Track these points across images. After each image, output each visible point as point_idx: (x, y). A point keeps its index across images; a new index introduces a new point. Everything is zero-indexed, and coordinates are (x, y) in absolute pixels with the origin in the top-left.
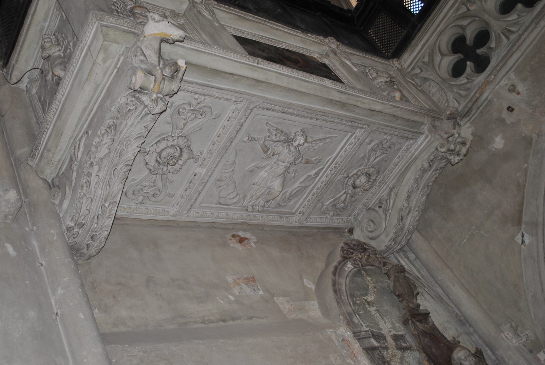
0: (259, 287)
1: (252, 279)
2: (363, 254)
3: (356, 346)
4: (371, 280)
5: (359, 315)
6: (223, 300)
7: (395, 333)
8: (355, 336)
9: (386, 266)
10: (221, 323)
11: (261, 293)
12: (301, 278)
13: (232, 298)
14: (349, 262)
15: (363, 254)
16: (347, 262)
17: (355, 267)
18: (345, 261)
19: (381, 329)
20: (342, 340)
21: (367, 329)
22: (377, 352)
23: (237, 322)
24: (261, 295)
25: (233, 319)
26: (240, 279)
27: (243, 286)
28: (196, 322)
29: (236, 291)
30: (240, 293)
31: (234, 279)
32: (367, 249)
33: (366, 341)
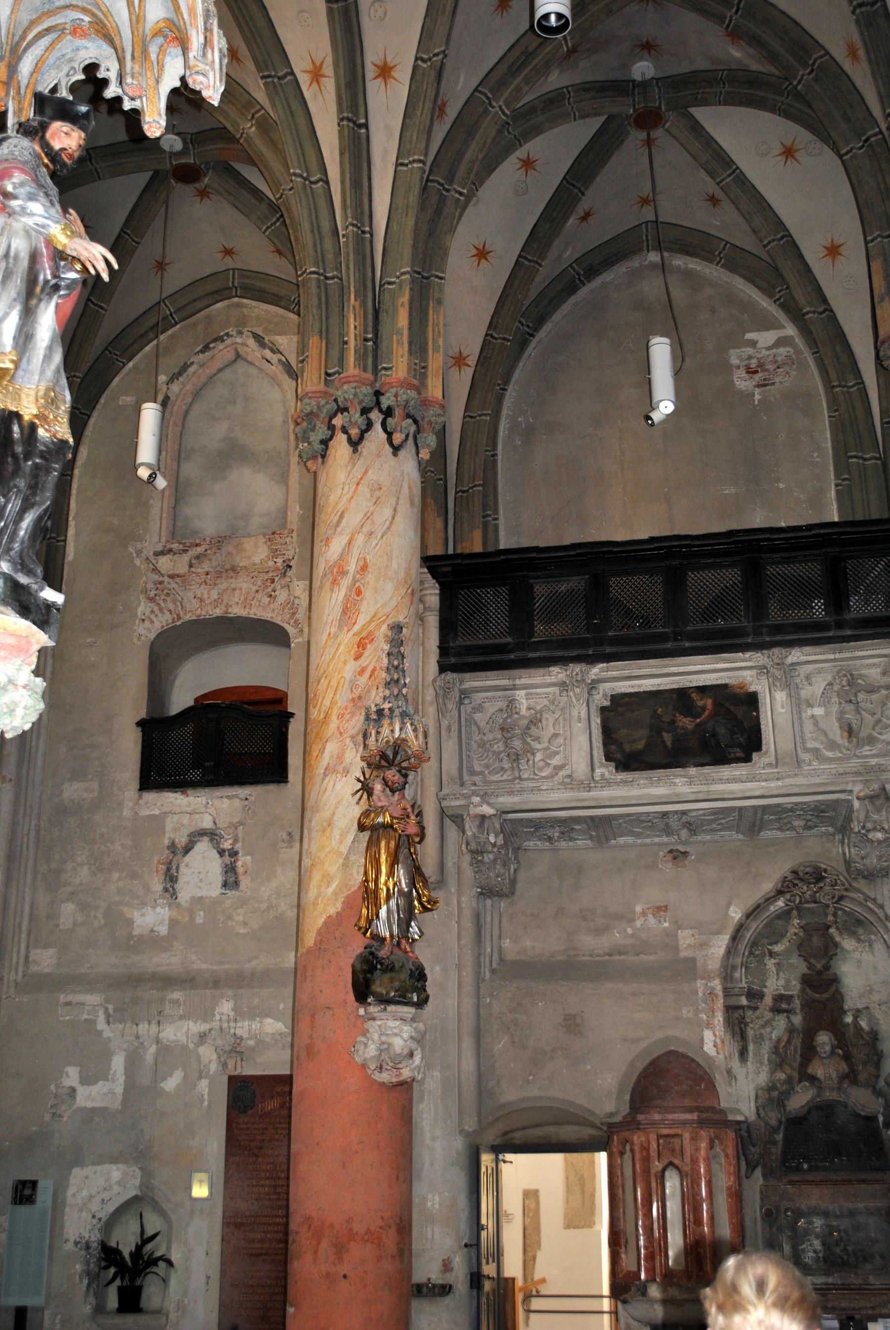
3: (720, 1003)
5: (746, 969)
6: (619, 933)
7: (783, 992)
8: (724, 992)
9: (842, 903)
10: (607, 958)
11: (666, 925)
12: (729, 905)
13: (629, 931)
19: (765, 987)
20: (710, 994)
21: (745, 986)
22: (741, 1012)
23: (622, 957)
24: (665, 928)
25: (620, 954)
27: (650, 917)
28: (584, 955)
29: (638, 924)
32: (825, 878)
33: (734, 998)
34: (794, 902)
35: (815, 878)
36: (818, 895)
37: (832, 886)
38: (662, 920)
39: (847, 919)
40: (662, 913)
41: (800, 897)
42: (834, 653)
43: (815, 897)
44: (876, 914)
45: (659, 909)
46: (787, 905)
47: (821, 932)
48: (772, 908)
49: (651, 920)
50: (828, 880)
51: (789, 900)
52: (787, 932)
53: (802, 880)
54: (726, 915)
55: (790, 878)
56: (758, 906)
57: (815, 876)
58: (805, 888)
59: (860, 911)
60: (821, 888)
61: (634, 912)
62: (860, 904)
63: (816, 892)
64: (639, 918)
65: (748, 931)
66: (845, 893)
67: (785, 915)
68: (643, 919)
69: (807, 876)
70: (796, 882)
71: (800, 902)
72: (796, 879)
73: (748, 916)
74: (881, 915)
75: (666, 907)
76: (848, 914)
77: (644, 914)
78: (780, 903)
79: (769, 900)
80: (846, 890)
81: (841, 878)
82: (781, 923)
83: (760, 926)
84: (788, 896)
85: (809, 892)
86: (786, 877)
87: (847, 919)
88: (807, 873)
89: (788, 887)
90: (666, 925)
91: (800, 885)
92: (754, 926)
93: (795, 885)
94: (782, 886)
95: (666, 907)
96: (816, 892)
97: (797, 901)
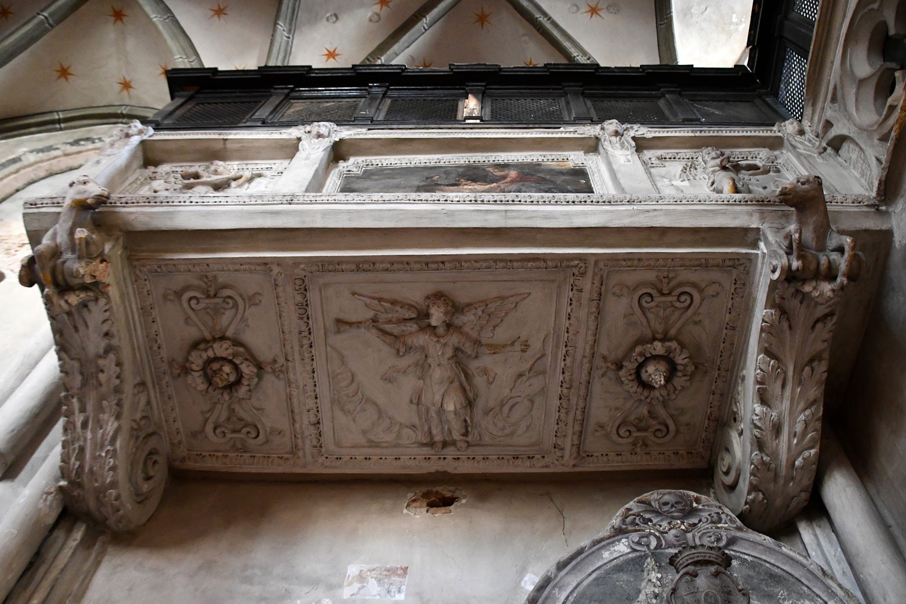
0: (403, 588)
1: (400, 572)
2: (679, 522)
4: (658, 579)
14: (624, 540)
15: (679, 522)
16: (619, 541)
17: (634, 550)
18: (616, 538)
26: (374, 570)
30: (353, 595)
31: (361, 571)
32: (700, 510)
34: (648, 546)
35: (681, 511)
36: (689, 535)
37: (712, 522)
38: (394, 589)
39: (751, 573)
40: (395, 579)
41: (658, 538)
42: (692, 131)
43: (686, 538)
44: (804, 566)
45: (392, 571)
46: (634, 550)
47: (713, 569)
48: (606, 555)
49: (373, 587)
50: (705, 515)
51: (639, 543)
52: (640, 591)
53: (657, 513)
54: (517, 585)
55: (635, 510)
56: (580, 552)
57: (680, 507)
58: (665, 524)
59: (772, 561)
60: (695, 525)
61: (344, 575)
62: (769, 550)
63: (686, 531)
64: (350, 584)
65: (561, 589)
66: (739, 534)
67: (634, 565)
68: (357, 585)
69: (665, 508)
70: (647, 516)
71: (659, 546)
72: (646, 511)
73: (561, 566)
74: (812, 567)
75: (405, 570)
76: (753, 566)
77: (361, 578)
78: (622, 547)
79: (599, 544)
80: (739, 529)
81: (727, 510)
82: (625, 577)
83: (585, 583)
84: (635, 537)
85: (673, 532)
86: (629, 510)
87: (751, 573)
88: (666, 504)
89: (633, 523)
90: (401, 597)
91: (655, 521)
92: (572, 581)
93: (647, 521)
94: (623, 521)
95: (405, 570)
96: (686, 531)
97: (654, 543)
